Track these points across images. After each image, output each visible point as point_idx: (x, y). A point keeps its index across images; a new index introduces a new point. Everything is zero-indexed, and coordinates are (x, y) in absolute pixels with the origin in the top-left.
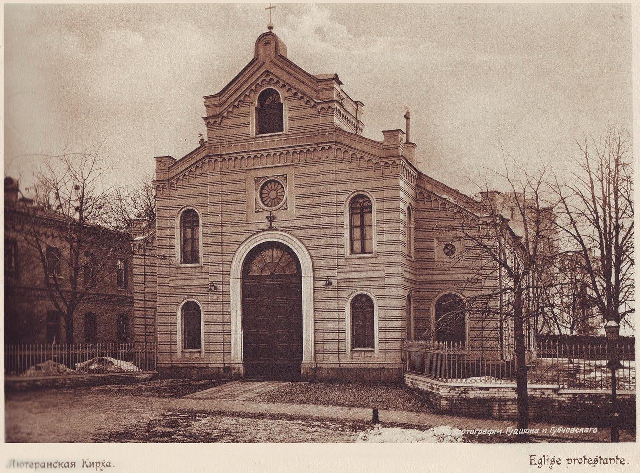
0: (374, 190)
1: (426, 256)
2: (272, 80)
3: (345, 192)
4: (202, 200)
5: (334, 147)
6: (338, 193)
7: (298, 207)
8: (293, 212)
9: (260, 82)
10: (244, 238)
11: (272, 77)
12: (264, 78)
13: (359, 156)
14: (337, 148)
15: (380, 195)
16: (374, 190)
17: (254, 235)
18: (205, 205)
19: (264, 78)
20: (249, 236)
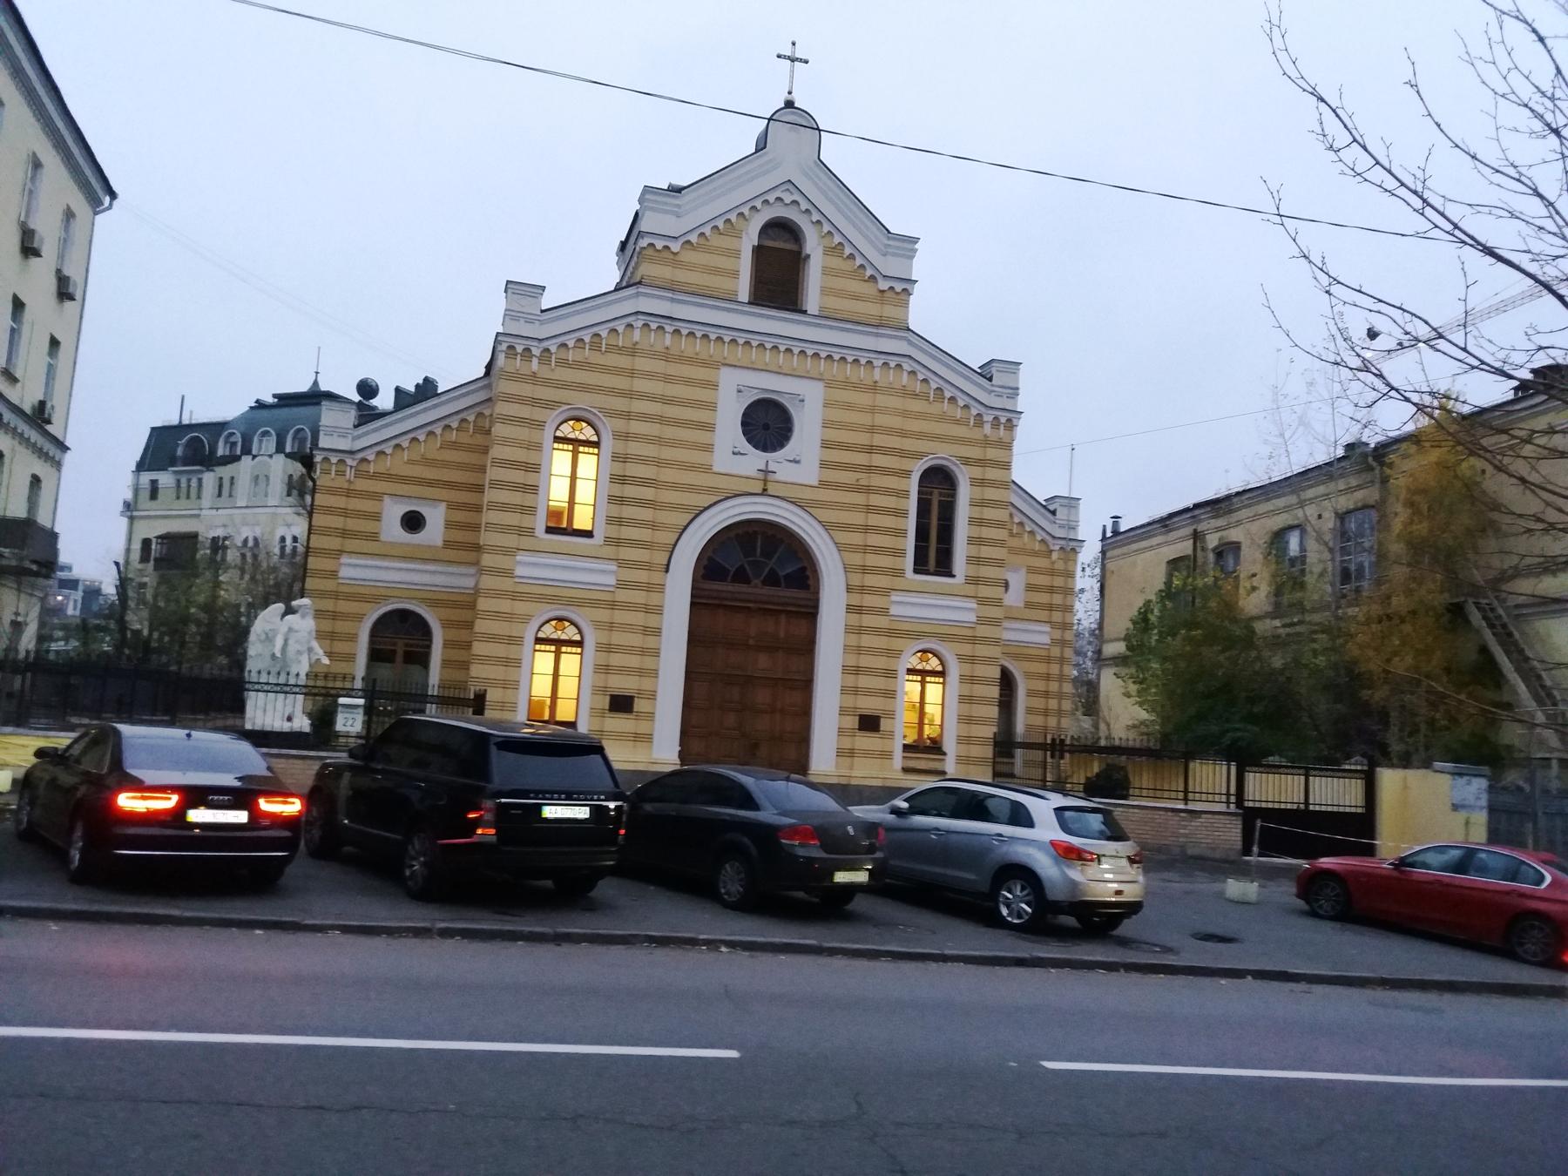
0: (967, 461)
1: (460, 516)
2: (795, 202)
3: (919, 455)
4: (620, 404)
5: (905, 366)
6: (902, 454)
7: (824, 465)
8: (808, 473)
10: (705, 500)
11: (797, 197)
12: (778, 194)
13: (948, 395)
14: (910, 370)
15: (977, 472)
16: (967, 461)
17: (727, 498)
18: (627, 416)
19: (778, 194)
20: (716, 499)
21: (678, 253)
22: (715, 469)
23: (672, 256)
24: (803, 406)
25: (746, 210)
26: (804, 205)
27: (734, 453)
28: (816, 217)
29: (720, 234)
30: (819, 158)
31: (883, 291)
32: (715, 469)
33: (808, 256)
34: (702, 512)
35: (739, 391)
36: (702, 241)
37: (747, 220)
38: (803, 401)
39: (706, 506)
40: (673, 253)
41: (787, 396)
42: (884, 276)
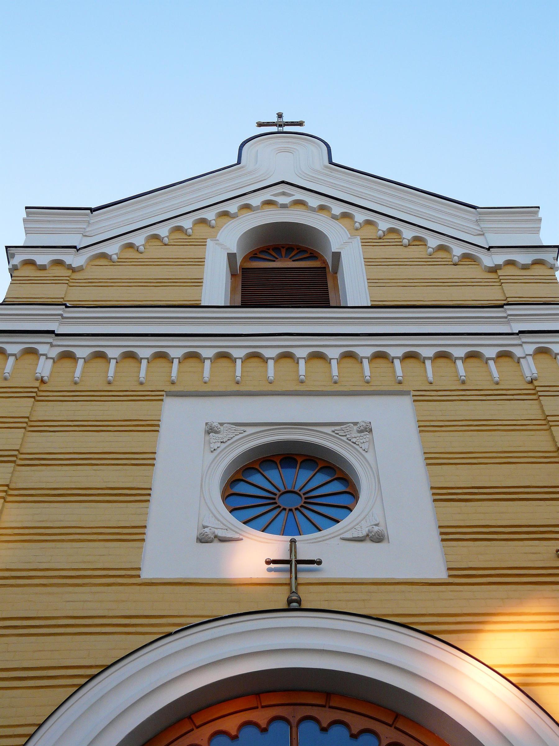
9: (256, 200)
12: (267, 195)
19: (267, 195)
21: (80, 269)
22: (146, 574)
23: (69, 273)
24: (372, 441)
25: (210, 215)
26: (314, 201)
27: (203, 540)
28: (337, 209)
29: (166, 245)
30: (331, 162)
31: (494, 270)
32: (146, 574)
33: (337, 256)
34: (93, 677)
35: (210, 430)
36: (130, 254)
37: (213, 227)
38: (368, 429)
39: (109, 664)
40: (74, 270)
41: (328, 430)
42: (489, 249)
